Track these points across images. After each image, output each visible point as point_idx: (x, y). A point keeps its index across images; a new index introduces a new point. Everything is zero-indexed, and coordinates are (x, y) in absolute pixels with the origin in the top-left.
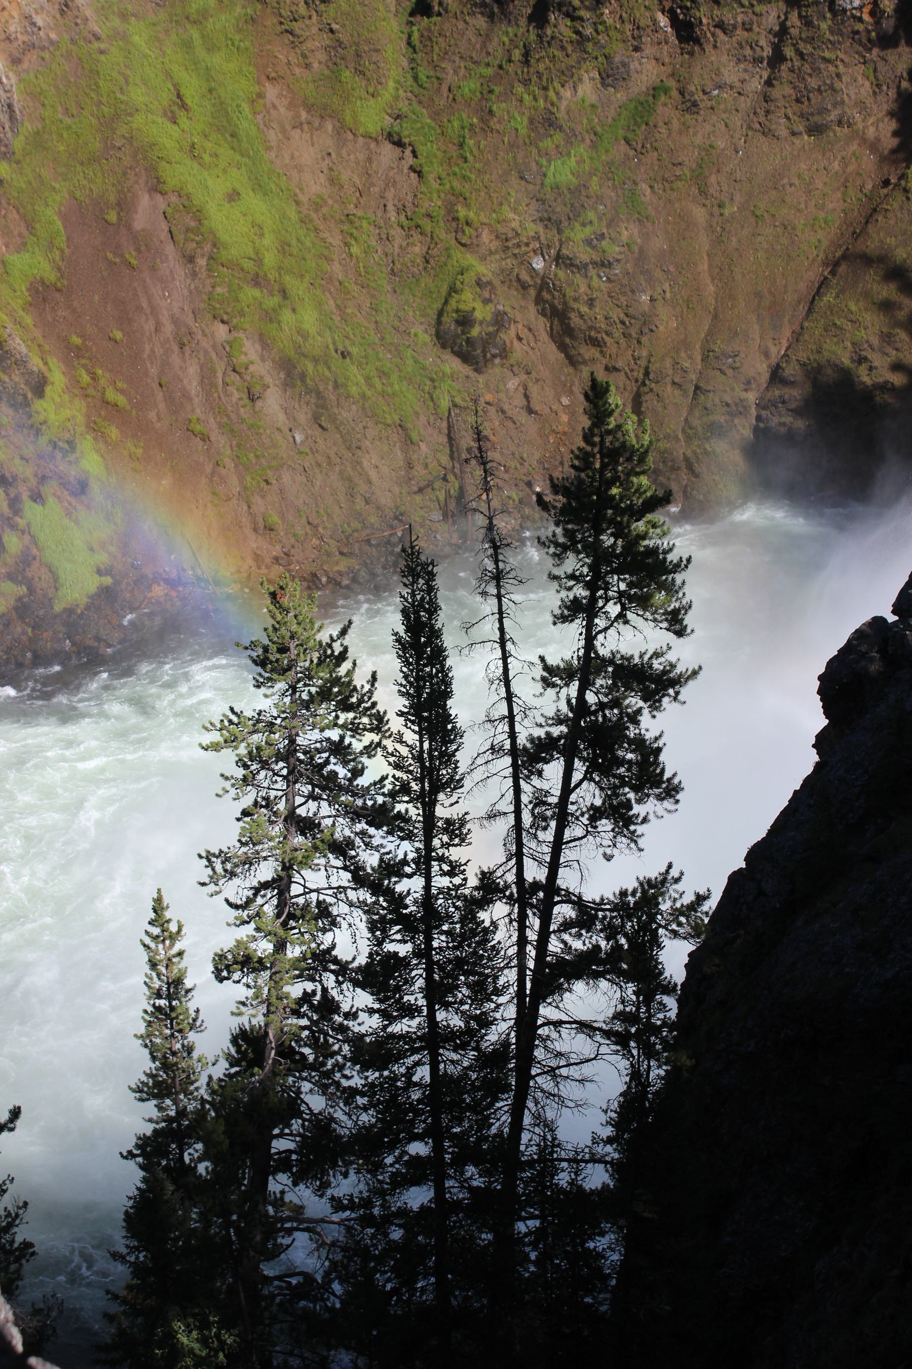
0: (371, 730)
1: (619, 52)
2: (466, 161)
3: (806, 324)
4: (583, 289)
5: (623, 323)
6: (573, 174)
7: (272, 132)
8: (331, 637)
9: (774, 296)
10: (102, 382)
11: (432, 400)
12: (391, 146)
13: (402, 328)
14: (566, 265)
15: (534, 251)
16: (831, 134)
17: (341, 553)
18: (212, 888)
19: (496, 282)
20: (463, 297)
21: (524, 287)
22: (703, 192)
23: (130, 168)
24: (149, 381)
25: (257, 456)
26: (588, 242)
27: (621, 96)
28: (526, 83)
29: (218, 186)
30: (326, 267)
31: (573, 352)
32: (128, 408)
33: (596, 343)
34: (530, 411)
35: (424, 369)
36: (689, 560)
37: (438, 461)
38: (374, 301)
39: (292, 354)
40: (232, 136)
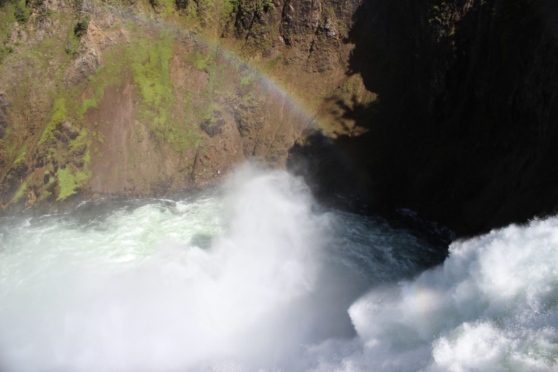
1: (267, 47)
26: (249, 101)
27: (268, 60)
28: (240, 55)
33: (247, 130)
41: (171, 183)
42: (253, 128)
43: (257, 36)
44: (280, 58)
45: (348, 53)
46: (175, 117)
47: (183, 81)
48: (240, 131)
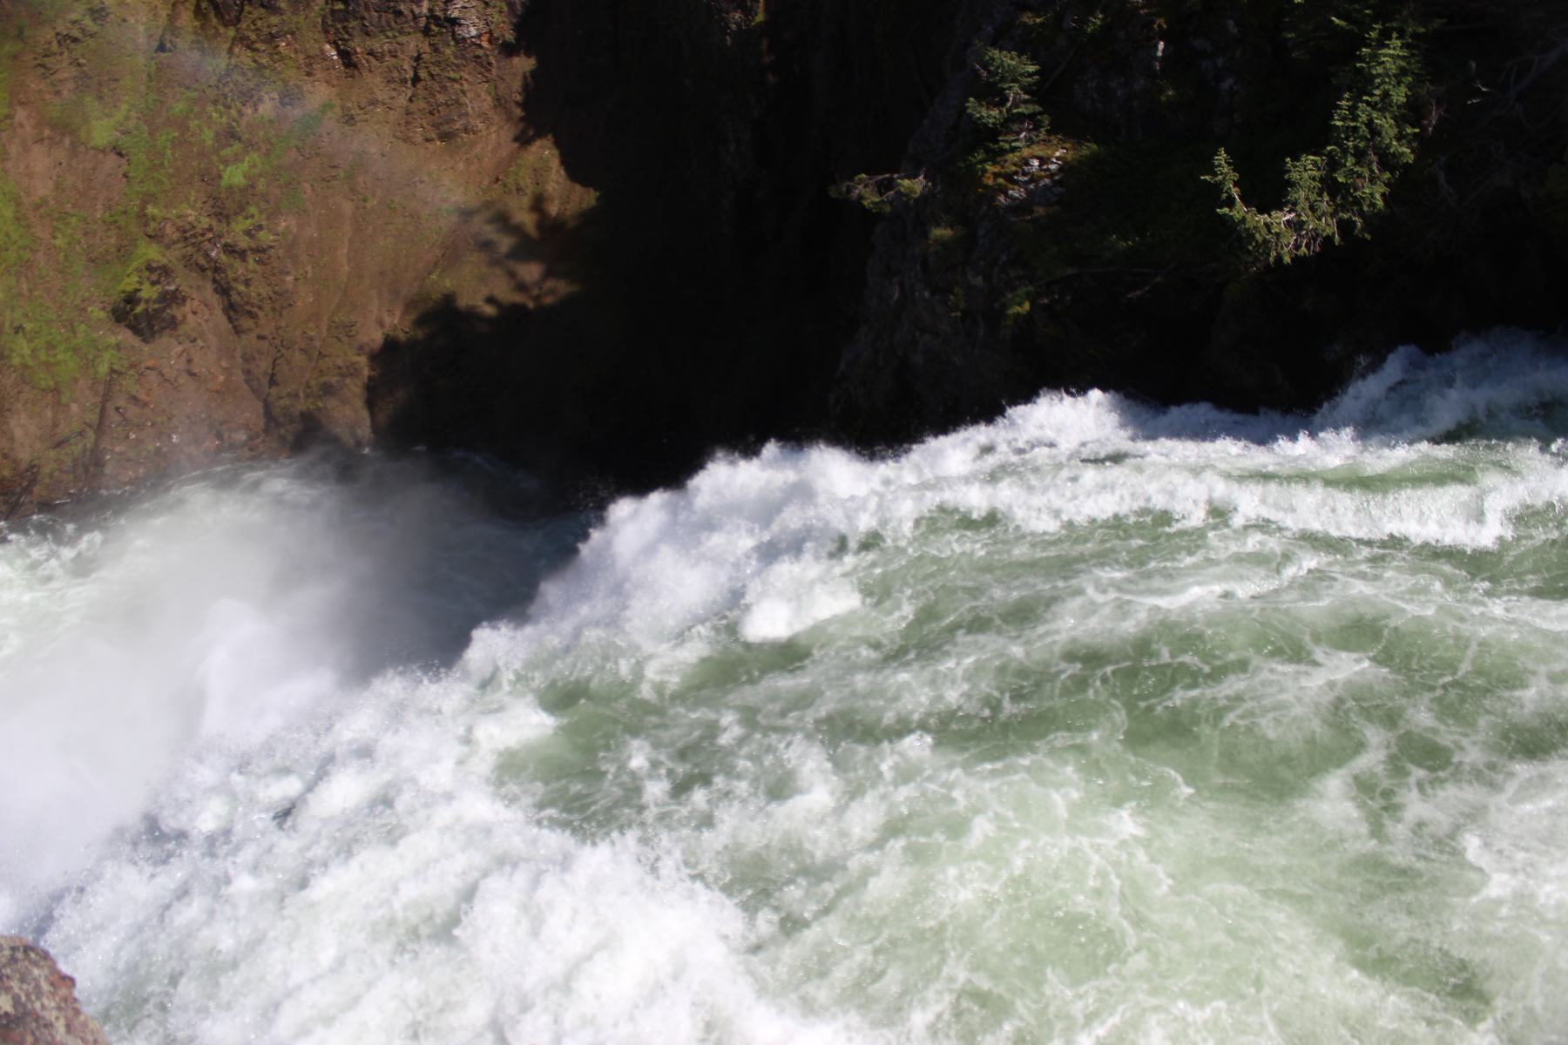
21: (203, 270)
26: (248, 233)
28: (215, 102)
41: (33, 481)
42: (267, 307)
43: (258, 45)
44: (332, 107)
45: (517, 85)
46: (30, 290)
47: (50, 184)
48: (230, 320)
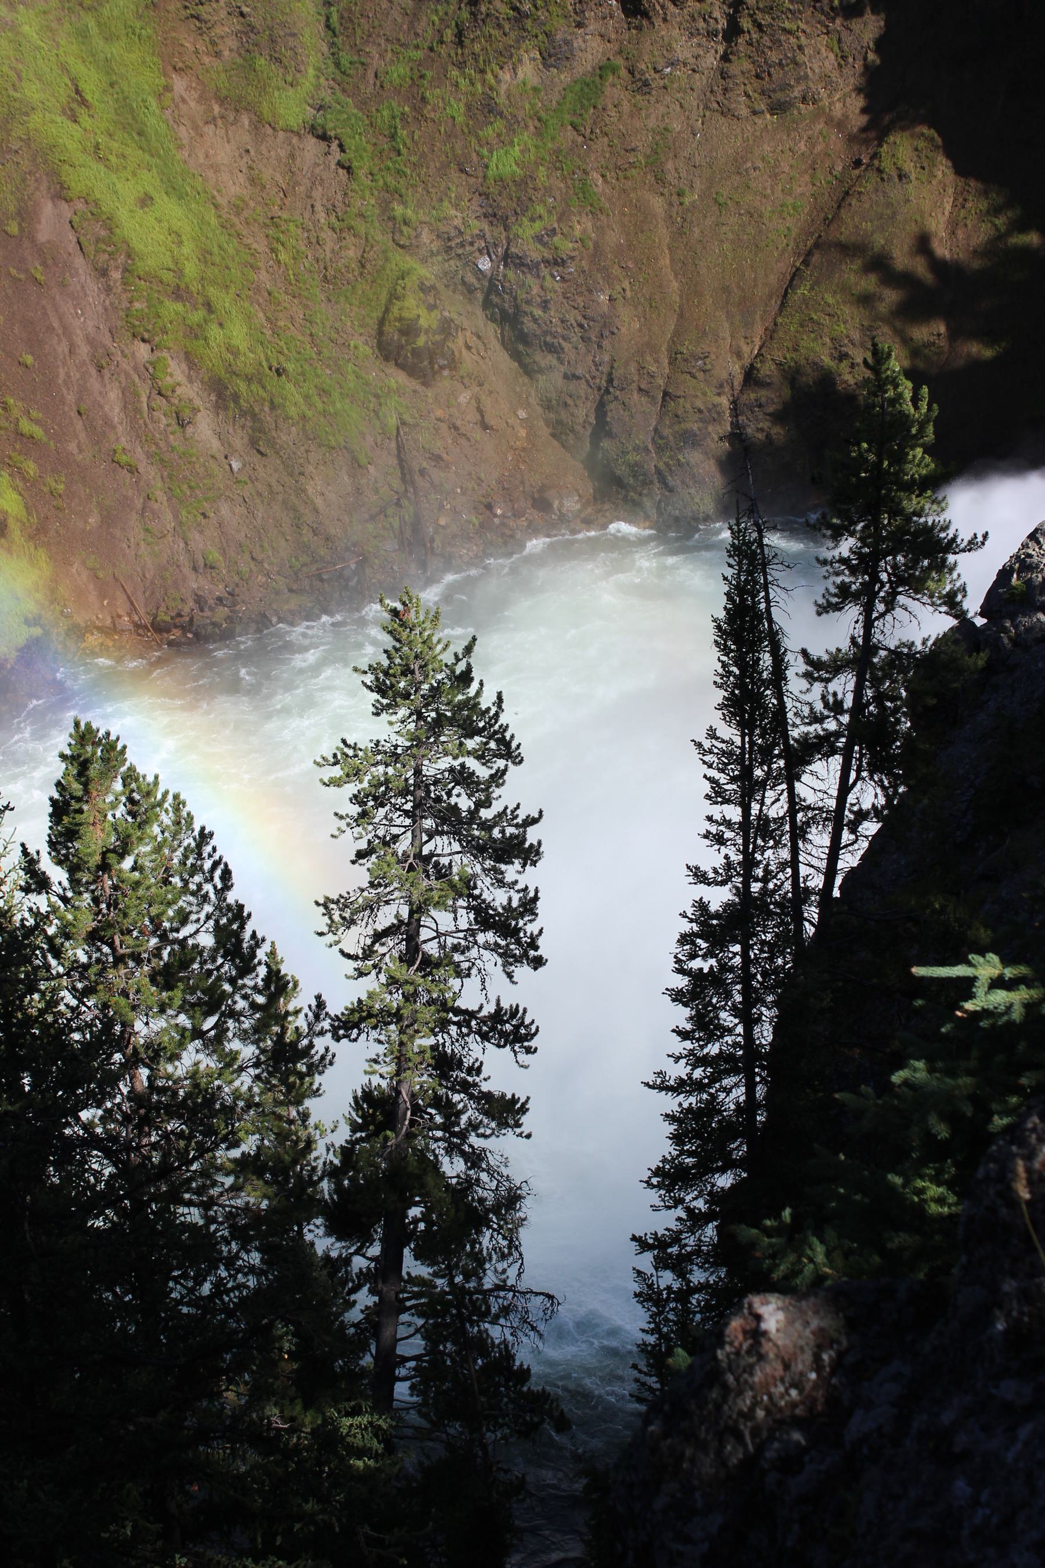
0: (501, 756)
2: (399, 154)
3: (780, 320)
4: (535, 290)
5: (581, 326)
6: (517, 164)
7: (182, 128)
8: (456, 655)
9: (743, 290)
10: (16, 412)
11: (378, 418)
12: (314, 140)
13: (340, 341)
14: (515, 265)
15: (480, 251)
16: (795, 112)
17: (291, 590)
18: (330, 938)
19: (441, 287)
20: (406, 304)
22: (660, 180)
23: (30, 173)
24: (66, 409)
25: (190, 487)
26: (539, 239)
27: (565, 77)
28: (461, 65)
29: (129, 190)
30: (252, 275)
31: (528, 360)
32: (45, 439)
34: (485, 426)
35: (367, 384)
36: (985, 536)
37: (390, 485)
38: (308, 312)
39: (223, 373)
40: (139, 134)
48: (516, 356)
